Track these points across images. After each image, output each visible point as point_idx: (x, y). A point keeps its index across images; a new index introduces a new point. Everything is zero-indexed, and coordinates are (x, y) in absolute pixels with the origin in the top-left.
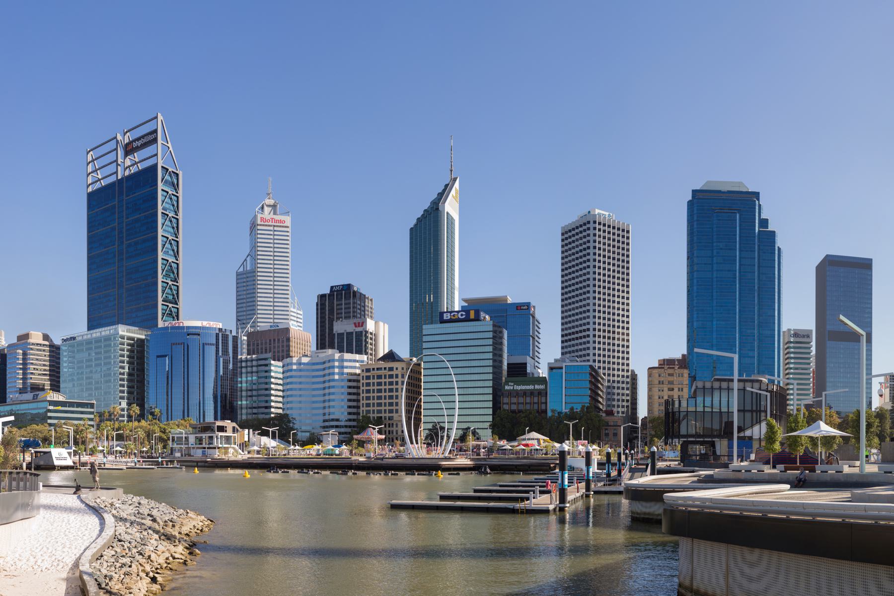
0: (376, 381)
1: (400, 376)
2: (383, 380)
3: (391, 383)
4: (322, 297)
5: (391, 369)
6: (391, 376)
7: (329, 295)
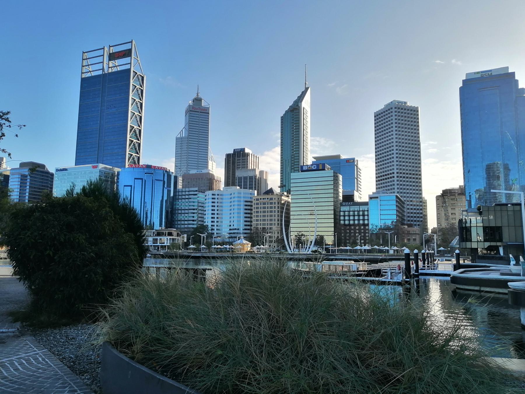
0: (262, 206)
1: (277, 203)
2: (266, 206)
4: (228, 156)
5: (271, 199)
6: (271, 203)
7: (233, 154)
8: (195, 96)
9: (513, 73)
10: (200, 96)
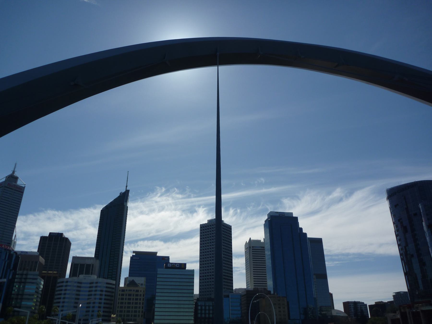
0: (128, 297)
2: (132, 297)
3: (137, 299)
5: (137, 291)
6: (137, 295)
8: (10, 173)
9: (296, 218)
10: (16, 174)
